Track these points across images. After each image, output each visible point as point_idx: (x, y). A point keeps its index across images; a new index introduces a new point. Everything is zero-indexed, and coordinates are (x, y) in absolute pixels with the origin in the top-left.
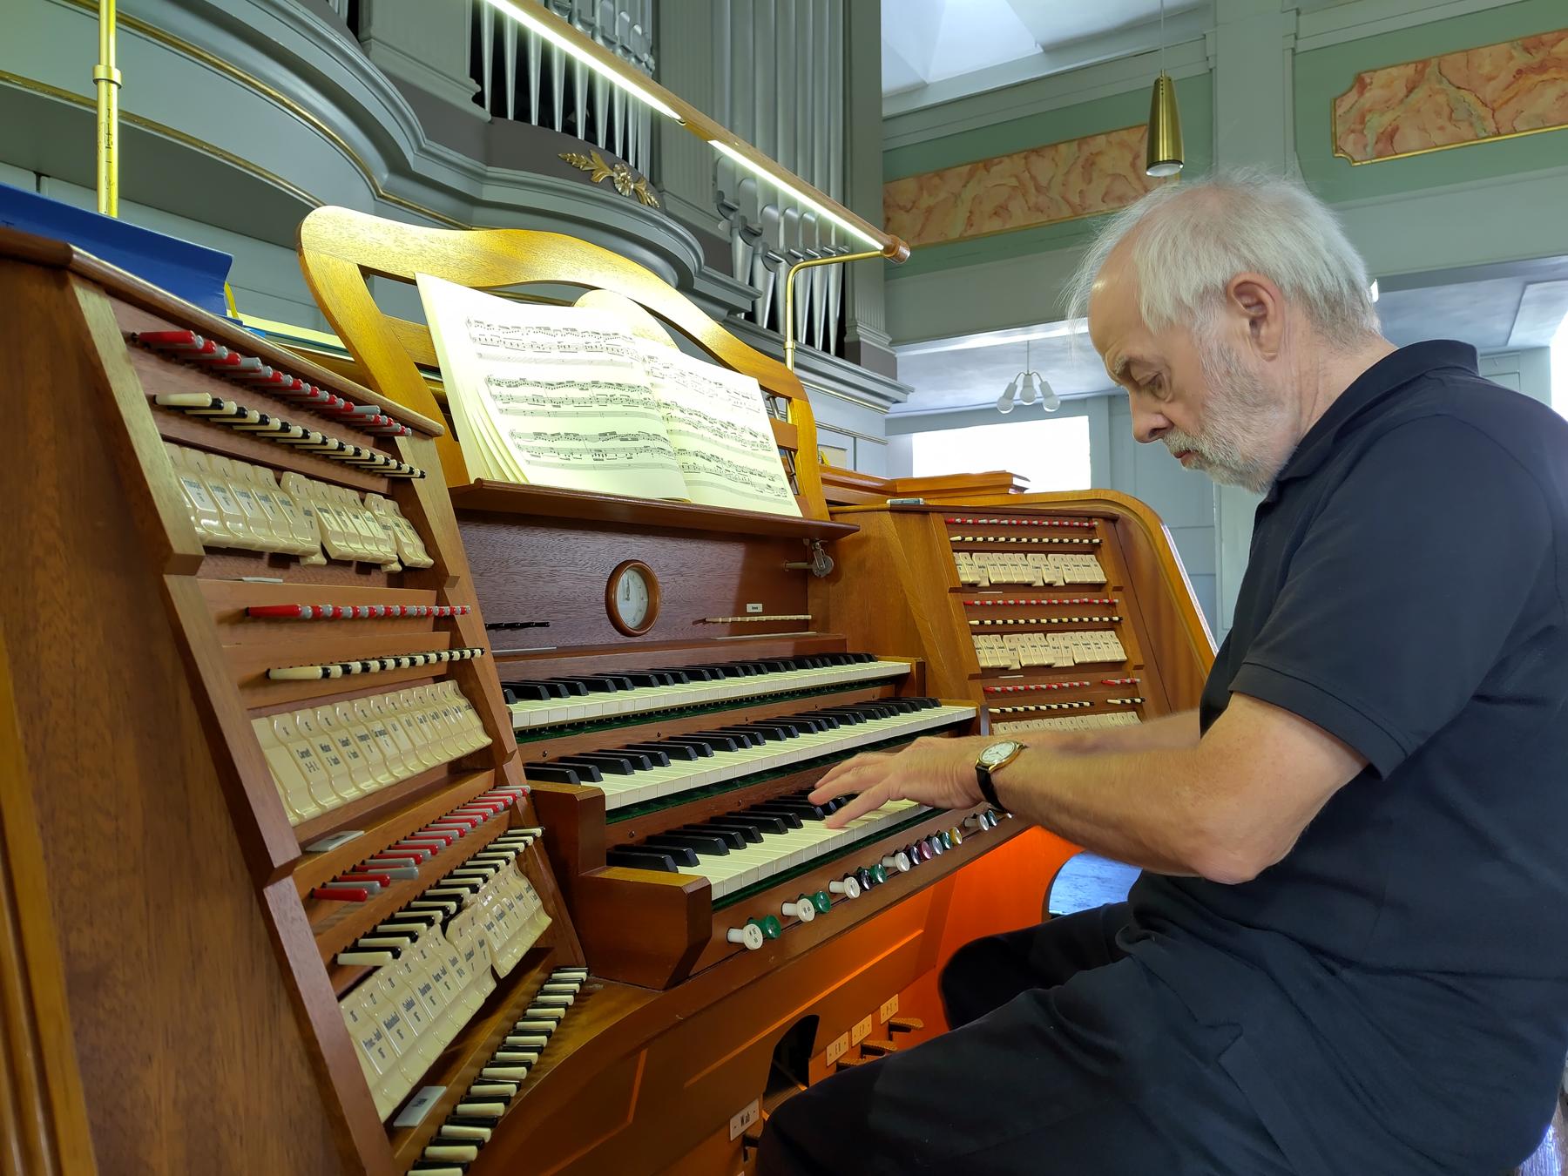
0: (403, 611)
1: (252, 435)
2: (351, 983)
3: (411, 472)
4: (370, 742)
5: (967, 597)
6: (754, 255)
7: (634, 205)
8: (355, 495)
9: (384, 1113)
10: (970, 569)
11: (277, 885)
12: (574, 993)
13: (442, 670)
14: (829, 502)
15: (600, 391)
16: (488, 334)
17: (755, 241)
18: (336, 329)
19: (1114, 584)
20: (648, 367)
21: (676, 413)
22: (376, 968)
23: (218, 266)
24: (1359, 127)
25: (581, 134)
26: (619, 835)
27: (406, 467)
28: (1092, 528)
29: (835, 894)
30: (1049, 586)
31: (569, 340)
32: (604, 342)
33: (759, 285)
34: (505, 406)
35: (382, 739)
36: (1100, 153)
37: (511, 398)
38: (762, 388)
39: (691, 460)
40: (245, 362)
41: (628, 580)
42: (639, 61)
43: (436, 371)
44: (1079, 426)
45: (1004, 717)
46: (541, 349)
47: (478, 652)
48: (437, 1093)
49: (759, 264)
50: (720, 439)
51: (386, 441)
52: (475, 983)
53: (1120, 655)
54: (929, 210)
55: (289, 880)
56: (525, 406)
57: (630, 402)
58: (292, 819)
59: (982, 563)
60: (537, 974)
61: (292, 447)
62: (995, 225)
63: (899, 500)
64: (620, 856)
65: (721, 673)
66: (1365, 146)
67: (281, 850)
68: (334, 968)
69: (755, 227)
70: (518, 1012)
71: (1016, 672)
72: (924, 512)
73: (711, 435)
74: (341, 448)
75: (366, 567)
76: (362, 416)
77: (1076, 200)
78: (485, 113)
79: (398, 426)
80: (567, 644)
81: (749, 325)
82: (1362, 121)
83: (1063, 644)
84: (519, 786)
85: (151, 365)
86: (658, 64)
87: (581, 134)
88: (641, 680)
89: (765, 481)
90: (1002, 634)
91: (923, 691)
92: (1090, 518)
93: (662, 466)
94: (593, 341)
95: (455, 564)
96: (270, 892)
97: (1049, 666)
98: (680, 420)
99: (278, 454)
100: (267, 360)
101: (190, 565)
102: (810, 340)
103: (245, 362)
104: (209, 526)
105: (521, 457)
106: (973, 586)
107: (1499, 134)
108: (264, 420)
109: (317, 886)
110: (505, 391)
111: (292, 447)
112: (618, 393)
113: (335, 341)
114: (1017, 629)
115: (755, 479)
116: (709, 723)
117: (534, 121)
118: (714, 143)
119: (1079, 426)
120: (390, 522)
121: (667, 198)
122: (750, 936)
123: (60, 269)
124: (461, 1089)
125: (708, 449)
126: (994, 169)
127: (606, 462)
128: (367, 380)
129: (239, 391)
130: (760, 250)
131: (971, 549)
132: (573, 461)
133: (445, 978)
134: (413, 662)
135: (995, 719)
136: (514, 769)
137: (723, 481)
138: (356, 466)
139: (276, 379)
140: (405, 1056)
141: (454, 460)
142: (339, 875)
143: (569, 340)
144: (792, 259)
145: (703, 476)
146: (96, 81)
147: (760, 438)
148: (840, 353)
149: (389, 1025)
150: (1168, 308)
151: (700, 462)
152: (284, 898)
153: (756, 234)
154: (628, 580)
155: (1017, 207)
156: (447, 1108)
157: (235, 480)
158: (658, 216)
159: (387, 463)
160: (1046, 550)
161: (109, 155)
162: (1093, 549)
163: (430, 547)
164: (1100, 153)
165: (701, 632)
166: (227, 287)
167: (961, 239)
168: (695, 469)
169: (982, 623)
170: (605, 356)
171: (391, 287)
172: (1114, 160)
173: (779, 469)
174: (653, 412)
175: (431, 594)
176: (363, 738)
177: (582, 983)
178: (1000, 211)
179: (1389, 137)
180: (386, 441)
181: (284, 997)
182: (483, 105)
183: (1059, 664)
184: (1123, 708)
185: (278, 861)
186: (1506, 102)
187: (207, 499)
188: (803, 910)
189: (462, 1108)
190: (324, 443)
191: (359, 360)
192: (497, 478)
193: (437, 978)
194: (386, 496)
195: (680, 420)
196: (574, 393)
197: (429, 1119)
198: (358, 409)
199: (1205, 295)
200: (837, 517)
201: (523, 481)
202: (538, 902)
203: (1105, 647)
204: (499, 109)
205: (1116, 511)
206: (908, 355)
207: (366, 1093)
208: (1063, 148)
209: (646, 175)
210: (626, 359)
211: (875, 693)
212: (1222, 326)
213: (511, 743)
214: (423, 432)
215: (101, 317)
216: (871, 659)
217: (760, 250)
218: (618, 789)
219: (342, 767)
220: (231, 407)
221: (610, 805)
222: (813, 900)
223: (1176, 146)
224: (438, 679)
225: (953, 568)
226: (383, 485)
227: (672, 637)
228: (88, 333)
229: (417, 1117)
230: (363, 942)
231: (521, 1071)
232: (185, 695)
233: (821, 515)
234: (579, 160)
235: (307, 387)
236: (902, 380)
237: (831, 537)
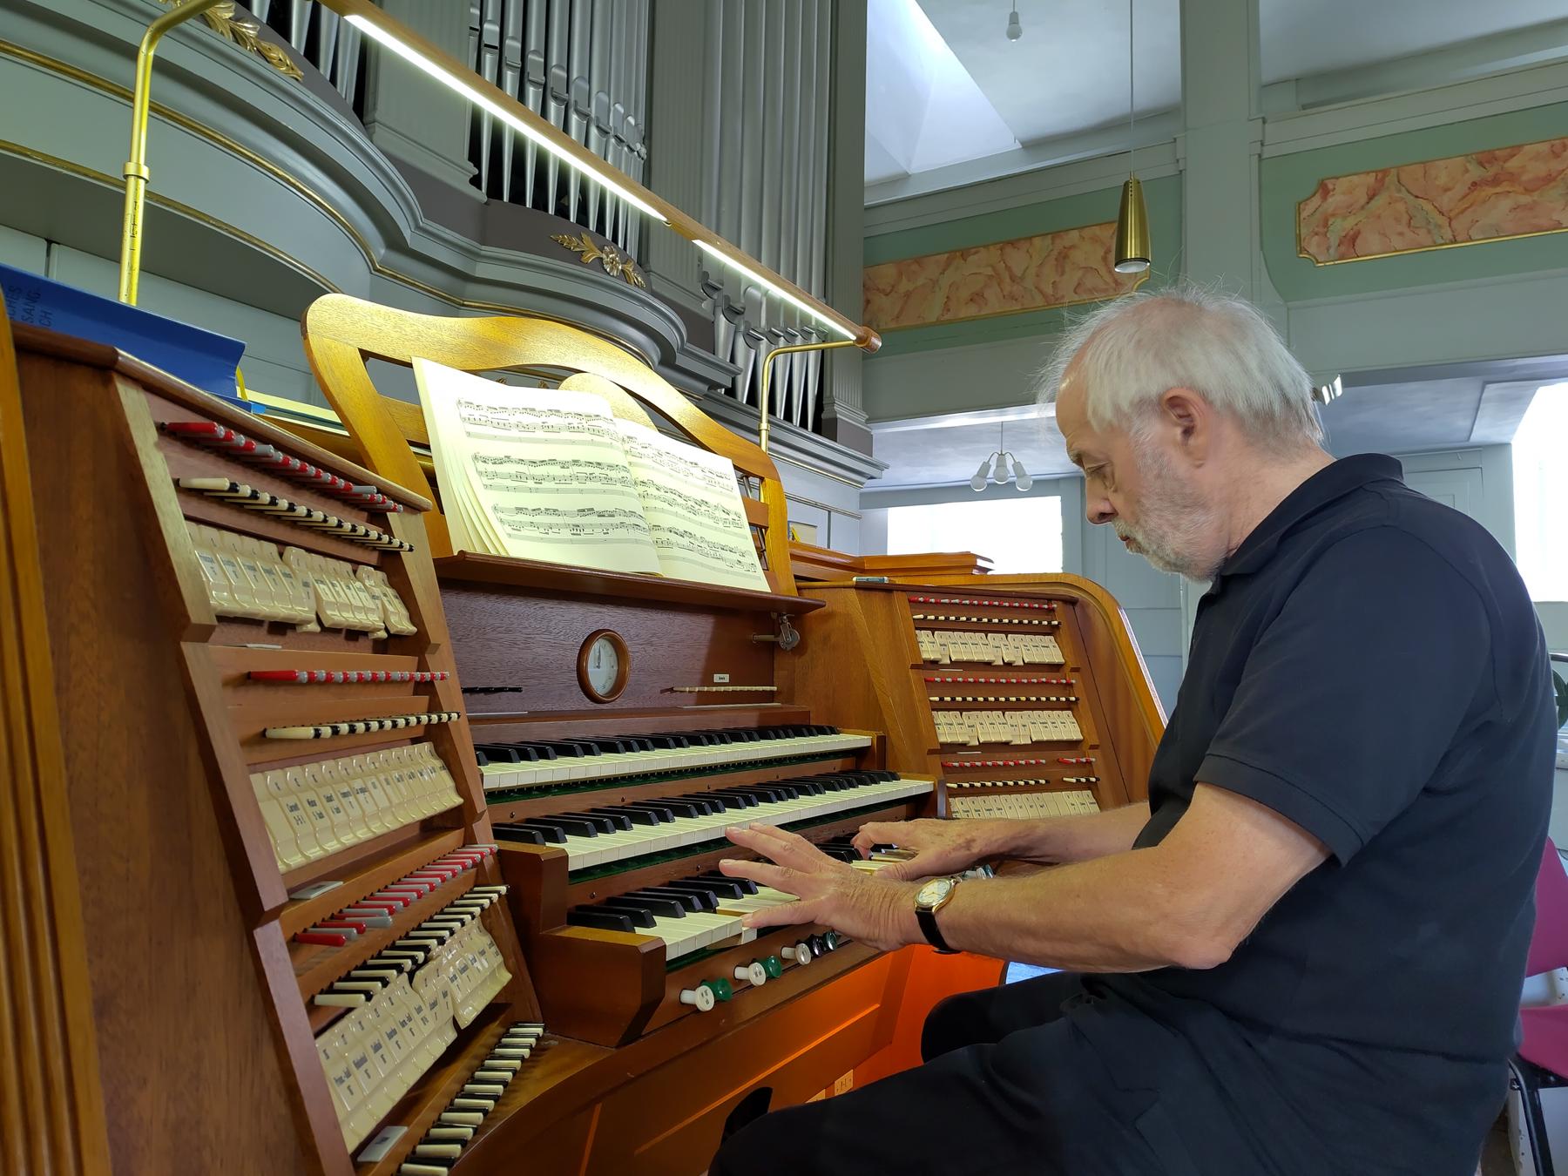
0: (388, 677)
1: (260, 514)
2: (324, 1024)
3: (401, 546)
4: (351, 799)
5: (929, 674)
7: (621, 284)
8: (348, 566)
9: (351, 1145)
10: (931, 646)
11: (266, 927)
12: (530, 1047)
13: (420, 732)
14: (797, 577)
16: (477, 414)
17: (737, 319)
18: (334, 406)
19: (1071, 665)
20: (627, 447)
22: (350, 1010)
23: (230, 352)
25: (573, 218)
26: (581, 895)
27: (396, 542)
28: (1053, 610)
29: (785, 961)
30: (1008, 665)
31: (553, 421)
32: (586, 423)
33: (740, 361)
35: (361, 796)
36: (1072, 247)
37: (495, 475)
38: (736, 467)
39: (665, 536)
40: (259, 448)
41: (601, 649)
42: (632, 150)
43: (427, 447)
44: (1051, 507)
46: (526, 428)
47: (454, 716)
48: (401, 1132)
49: (741, 341)
50: (693, 514)
51: (378, 516)
52: (439, 1032)
54: (908, 295)
55: (276, 924)
56: (508, 483)
57: (608, 479)
58: (282, 867)
59: (943, 641)
60: (495, 1028)
61: (295, 524)
62: (972, 310)
63: (865, 578)
64: (581, 916)
65: (685, 742)
67: (271, 896)
68: (311, 1007)
69: (738, 306)
70: (476, 1063)
71: (973, 748)
72: (888, 590)
73: (684, 512)
74: (340, 525)
75: (354, 634)
76: (359, 495)
77: (1049, 290)
78: (481, 195)
79: (391, 503)
80: (538, 709)
81: (730, 400)
83: (1020, 722)
84: (487, 845)
85: (178, 452)
86: (649, 153)
87: (573, 218)
88: (608, 747)
89: (736, 557)
90: (961, 711)
91: (883, 762)
92: (1049, 600)
93: (636, 541)
94: (575, 422)
95: (437, 631)
96: (259, 933)
97: (1007, 744)
98: (656, 498)
99: (282, 531)
100: (279, 446)
101: (204, 634)
102: (788, 416)
103: (259, 448)
104: (221, 599)
106: (935, 663)
108: (273, 501)
109: (299, 931)
110: (490, 467)
111: (295, 524)
112: (597, 471)
113: (331, 416)
114: (976, 707)
116: (672, 789)
117: (529, 204)
118: (698, 242)
119: (1051, 507)
120: (377, 592)
121: (653, 278)
122: (702, 998)
123: (106, 369)
124: (422, 1132)
125: (682, 526)
126: (971, 258)
128: (361, 458)
129: (250, 473)
131: (933, 628)
133: (410, 1025)
134: (395, 725)
135: (953, 793)
136: (483, 828)
138: (352, 540)
139: (286, 462)
140: (370, 1096)
141: (439, 533)
142: (319, 922)
143: (553, 421)
144: (773, 338)
145: (676, 552)
146: (126, 177)
147: (732, 516)
148: (817, 429)
149: (359, 1064)
150: (1108, 414)
151: (674, 538)
152: (271, 939)
153: (738, 313)
154: (601, 649)
155: (992, 294)
156: (409, 1149)
157: (242, 554)
159: (379, 538)
160: (1007, 630)
161: (133, 243)
162: (1051, 631)
163: (414, 615)
164: (1072, 247)
165: (669, 701)
166: (238, 371)
167: (939, 323)
168: (668, 544)
169: (942, 699)
170: (587, 436)
171: (391, 371)
172: (1088, 251)
173: (749, 545)
174: (631, 490)
175: (413, 660)
176: (345, 795)
177: (538, 1038)
178: (976, 298)
179: (1351, 240)
180: (378, 516)
181: (267, 1031)
182: (479, 187)
183: (1016, 742)
184: (1078, 786)
185: (268, 904)
187: (223, 573)
188: (755, 974)
189: (422, 1148)
190: (325, 521)
191: (354, 435)
192: (479, 550)
193: (403, 1024)
194: (376, 568)
195: (656, 498)
196: (555, 470)
197: (389, 1158)
198: (356, 489)
199: (1141, 404)
200: (805, 592)
201: (503, 554)
202: (500, 959)
203: (1062, 727)
204: (495, 191)
205: (1075, 594)
206: (883, 432)
207: (336, 1126)
208: (1037, 241)
209: (634, 257)
210: (606, 439)
211: (836, 765)
212: (1155, 432)
213: (481, 804)
214: (413, 508)
215: (140, 414)
216: (833, 731)
218: (582, 850)
219: (325, 822)
220: (245, 490)
221: (573, 866)
222: (765, 964)
224: (415, 741)
225: (915, 646)
226: (373, 558)
227: (640, 705)
228: (127, 426)
229: (380, 1153)
230: (338, 985)
231: (478, 1117)
232: (193, 752)
233: (788, 590)
235: (312, 470)
236: (877, 456)
237: (798, 612)
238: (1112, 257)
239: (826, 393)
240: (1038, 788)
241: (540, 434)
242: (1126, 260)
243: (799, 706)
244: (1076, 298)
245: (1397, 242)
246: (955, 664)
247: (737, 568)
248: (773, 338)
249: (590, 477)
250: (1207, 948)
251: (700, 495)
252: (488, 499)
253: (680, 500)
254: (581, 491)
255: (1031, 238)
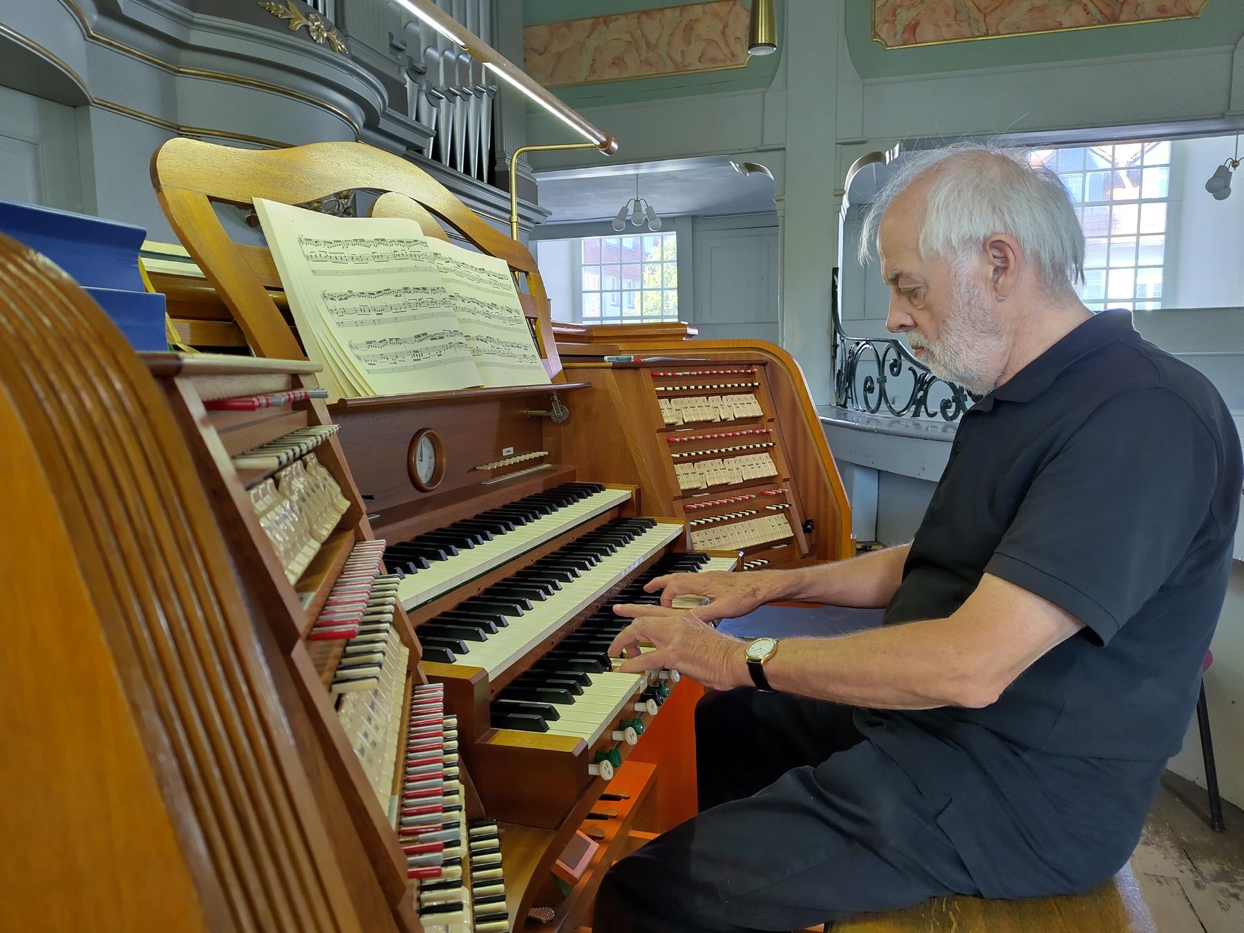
6: (419, 91)
10: (675, 412)
15: (411, 296)
17: (423, 80)
21: (459, 303)
24: (891, 19)
28: (753, 373)
30: (724, 422)
31: (381, 250)
34: (340, 320)
36: (697, 20)
43: (282, 290)
44: (671, 239)
45: (700, 527)
46: (360, 259)
49: (423, 99)
53: (772, 471)
54: (559, 55)
66: (895, 34)
69: (420, 66)
71: (704, 491)
72: (636, 367)
77: (678, 58)
82: (894, 15)
89: (521, 352)
92: (750, 365)
98: (464, 309)
102: (467, 170)
105: (361, 367)
106: (672, 427)
107: (987, 35)
110: (338, 304)
114: (706, 457)
115: (515, 351)
118: (489, 65)
119: (671, 239)
121: (351, 42)
126: (612, 25)
127: (423, 361)
130: (424, 87)
131: (670, 396)
132: (399, 364)
135: (693, 529)
137: (496, 359)
143: (381, 250)
144: (451, 96)
145: (485, 358)
148: (491, 181)
151: (481, 345)
153: (421, 73)
158: (351, 65)
160: (722, 393)
162: (752, 390)
163: (346, 493)
164: (697, 20)
170: (410, 263)
172: (708, 27)
179: (913, 28)
184: (778, 511)
186: (994, 10)
195: (464, 309)
201: (371, 395)
203: (763, 466)
205: (767, 356)
206: (541, 178)
208: (667, 12)
209: (332, 20)
211: (608, 517)
217: (424, 87)
223: (771, 32)
234: (278, 9)
236: (542, 204)
238: (745, 41)
239: (498, 148)
240: (751, 517)
241: (372, 265)
242: (758, 45)
243: (567, 467)
244: (700, 66)
245: (946, 33)
246: (687, 425)
247: (525, 363)
248: (451, 96)
249: (420, 303)
250: (981, 693)
251: (488, 299)
252: (343, 337)
253: (479, 308)
254: (415, 317)
255: (662, 9)
